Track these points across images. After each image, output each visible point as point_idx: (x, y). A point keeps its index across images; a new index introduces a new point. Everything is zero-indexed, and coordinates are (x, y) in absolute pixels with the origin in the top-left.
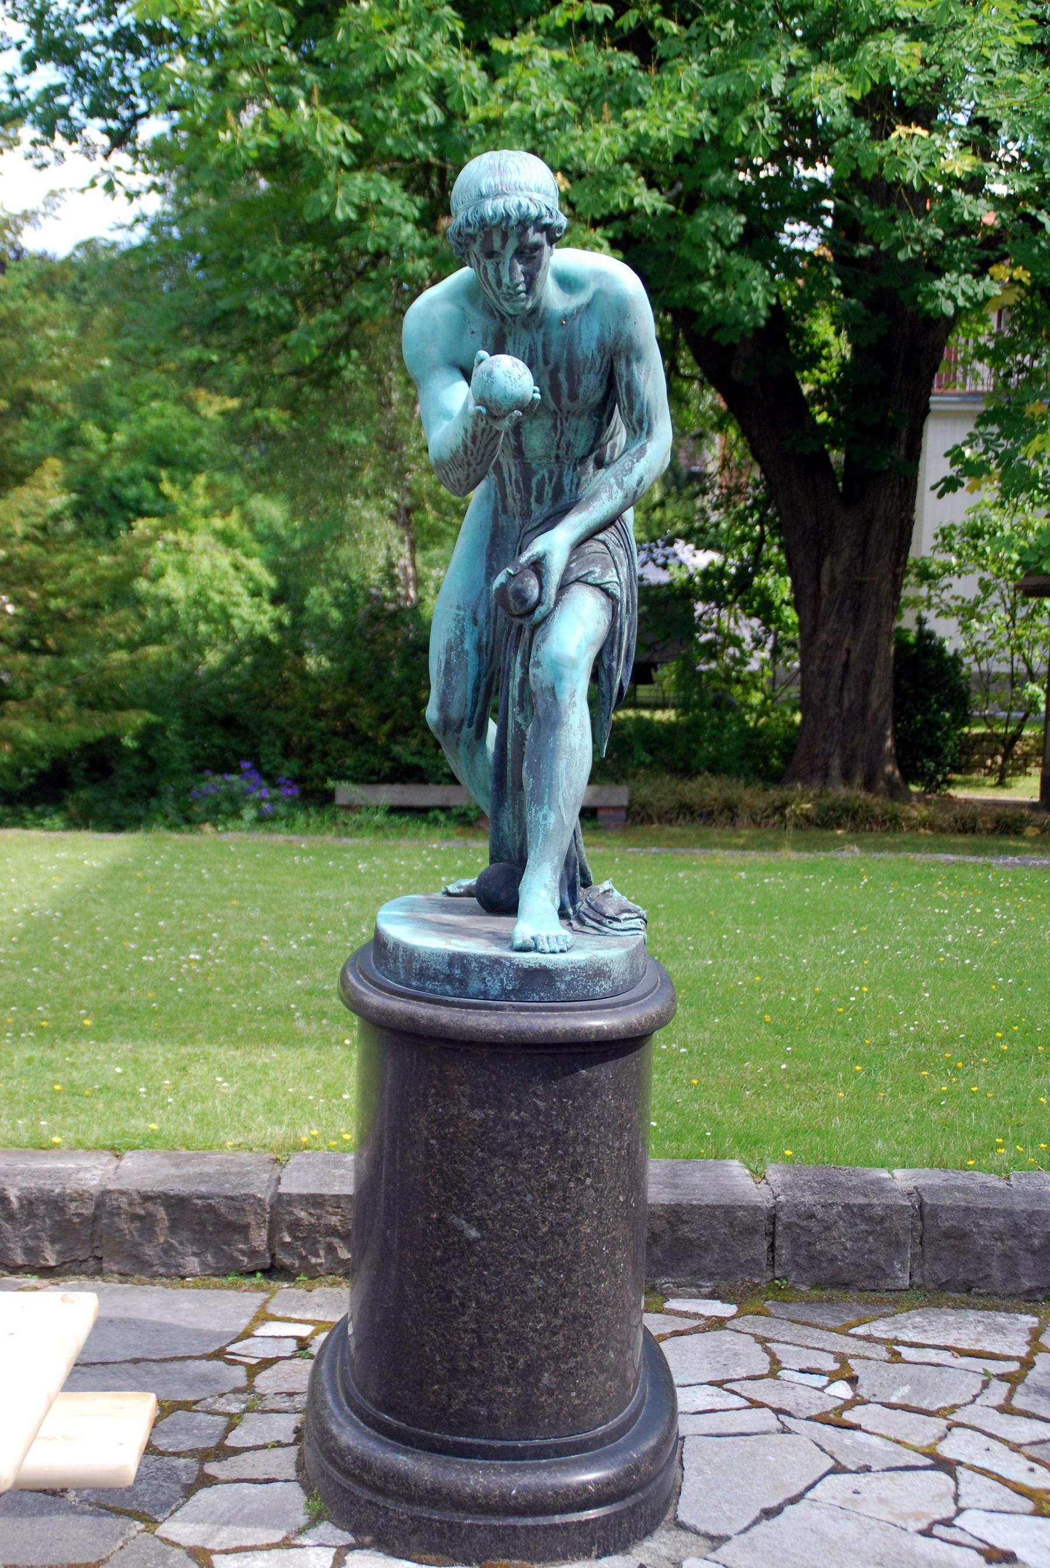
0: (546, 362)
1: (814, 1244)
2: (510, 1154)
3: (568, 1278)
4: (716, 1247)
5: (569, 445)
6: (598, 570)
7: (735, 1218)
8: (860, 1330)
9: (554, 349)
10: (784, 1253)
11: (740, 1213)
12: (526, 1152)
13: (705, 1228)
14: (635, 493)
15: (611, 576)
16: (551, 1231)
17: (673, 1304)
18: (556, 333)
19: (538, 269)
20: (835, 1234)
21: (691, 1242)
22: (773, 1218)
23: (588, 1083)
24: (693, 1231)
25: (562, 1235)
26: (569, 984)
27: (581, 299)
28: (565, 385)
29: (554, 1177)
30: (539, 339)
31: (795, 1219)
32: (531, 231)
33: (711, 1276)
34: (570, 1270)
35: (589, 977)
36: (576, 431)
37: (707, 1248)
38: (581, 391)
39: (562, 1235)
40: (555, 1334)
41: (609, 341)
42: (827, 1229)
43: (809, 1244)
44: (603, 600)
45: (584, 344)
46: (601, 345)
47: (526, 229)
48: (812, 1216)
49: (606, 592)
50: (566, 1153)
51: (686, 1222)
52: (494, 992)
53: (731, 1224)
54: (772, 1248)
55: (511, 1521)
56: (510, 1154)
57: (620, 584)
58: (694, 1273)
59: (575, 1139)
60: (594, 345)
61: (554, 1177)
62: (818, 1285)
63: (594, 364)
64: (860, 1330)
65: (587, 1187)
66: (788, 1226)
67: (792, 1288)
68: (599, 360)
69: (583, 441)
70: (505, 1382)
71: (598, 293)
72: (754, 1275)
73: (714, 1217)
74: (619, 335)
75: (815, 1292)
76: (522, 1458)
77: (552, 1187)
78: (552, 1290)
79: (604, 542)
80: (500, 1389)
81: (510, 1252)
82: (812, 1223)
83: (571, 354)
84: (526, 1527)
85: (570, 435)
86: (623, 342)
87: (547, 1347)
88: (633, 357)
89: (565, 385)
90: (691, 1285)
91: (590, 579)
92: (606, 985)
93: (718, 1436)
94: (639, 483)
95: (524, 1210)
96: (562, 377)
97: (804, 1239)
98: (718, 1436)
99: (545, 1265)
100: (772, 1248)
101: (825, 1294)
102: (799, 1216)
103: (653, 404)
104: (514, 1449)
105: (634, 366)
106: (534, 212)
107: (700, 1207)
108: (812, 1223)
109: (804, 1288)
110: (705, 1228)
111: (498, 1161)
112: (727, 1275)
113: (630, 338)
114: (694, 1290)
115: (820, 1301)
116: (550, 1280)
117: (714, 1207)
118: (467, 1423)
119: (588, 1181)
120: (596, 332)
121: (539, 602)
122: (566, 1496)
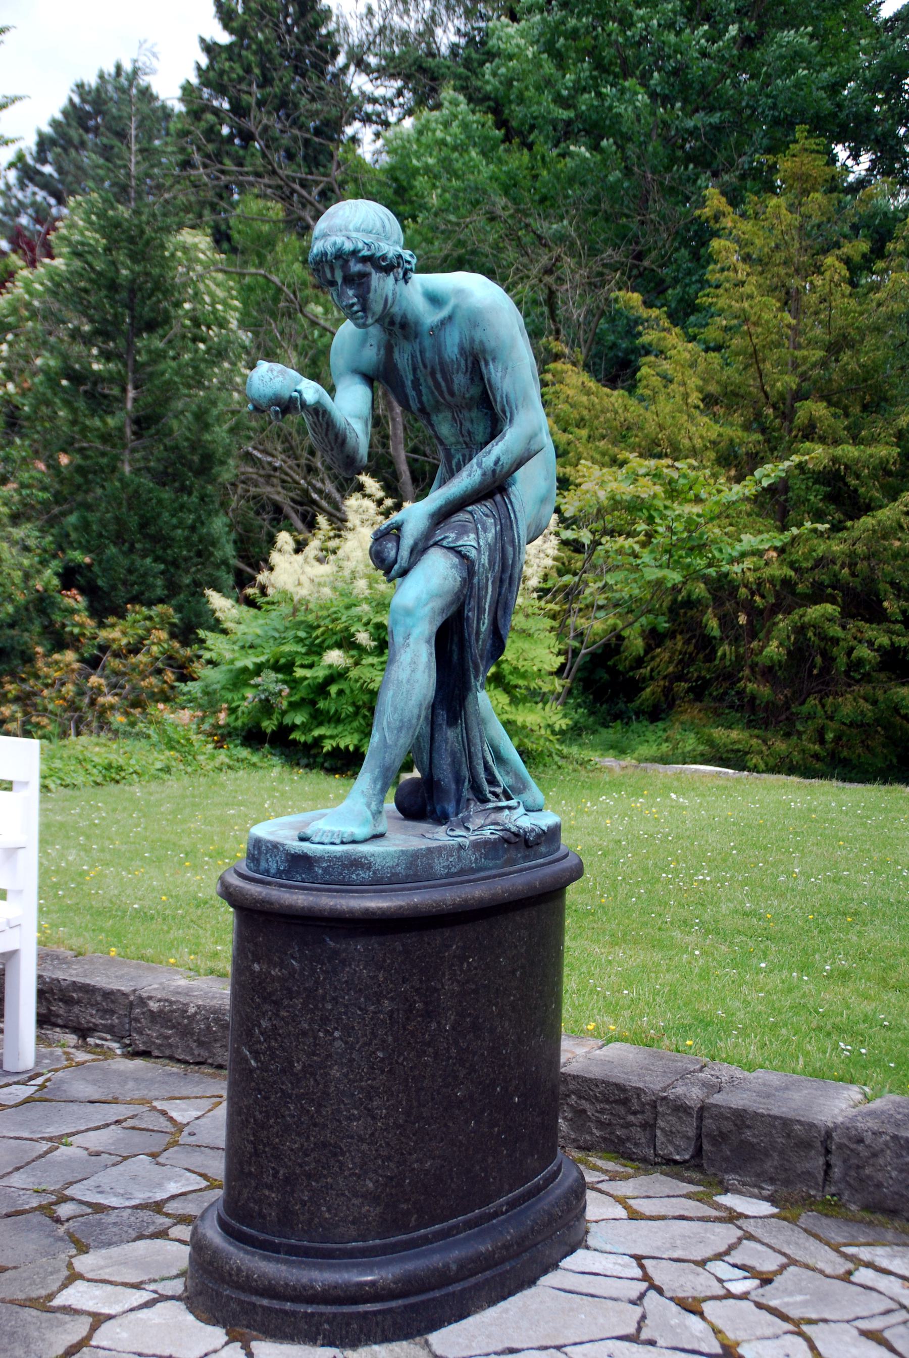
0: (425, 366)
1: (863, 1167)
2: (275, 1003)
3: (318, 1111)
4: (775, 1155)
5: (469, 433)
6: (452, 535)
7: (792, 1131)
8: (850, 1250)
9: (428, 355)
10: (837, 1172)
11: (797, 1127)
12: (286, 1002)
13: (765, 1135)
14: (494, 471)
15: (469, 540)
16: (304, 1069)
17: (728, 1200)
18: (427, 342)
19: (368, 292)
20: (881, 1161)
21: (752, 1145)
22: (828, 1135)
23: (335, 953)
24: (754, 1136)
25: (313, 1074)
26: (325, 870)
27: (444, 313)
28: (443, 384)
29: (306, 1026)
30: (417, 347)
31: (845, 1141)
32: (352, 263)
33: (772, 1181)
34: (320, 1105)
35: (344, 866)
36: (472, 421)
37: (767, 1155)
38: (456, 387)
39: (313, 1074)
40: (307, 1155)
41: (467, 345)
42: (875, 1155)
43: (858, 1167)
44: (456, 560)
45: (449, 350)
46: (462, 349)
47: (347, 261)
48: (861, 1141)
49: (458, 553)
50: (316, 1007)
51: (749, 1127)
52: (273, 871)
53: (789, 1136)
54: (828, 1166)
55: (254, 1299)
56: (275, 1003)
57: (478, 550)
58: (758, 1175)
59: (324, 997)
60: (456, 350)
61: (306, 1026)
62: (866, 1208)
63: (459, 365)
64: (850, 1250)
65: (335, 1039)
66: (841, 1146)
67: (844, 1205)
68: (463, 363)
69: (481, 429)
70: (270, 1187)
71: (456, 307)
72: (810, 1187)
73: (774, 1127)
74: (472, 340)
75: (863, 1214)
76: (278, 1252)
77: (304, 1033)
78: (304, 1118)
79: (471, 513)
80: (267, 1193)
81: (275, 1082)
82: (860, 1148)
83: (441, 358)
84: (262, 1306)
85: (467, 425)
86: (477, 346)
87: (301, 1166)
88: (489, 358)
89: (443, 384)
90: (755, 1186)
91: (445, 543)
92: (365, 875)
93: (592, 1296)
94: (496, 463)
95: (284, 1050)
96: (439, 376)
97: (854, 1161)
98: (592, 1296)
99: (300, 1097)
100: (828, 1166)
101: (867, 1216)
102: (850, 1139)
103: (512, 397)
104: (273, 1243)
105: (491, 366)
106: (348, 246)
107: (762, 1115)
108: (860, 1148)
109: (853, 1207)
110: (765, 1135)
111: (266, 1007)
112: (787, 1183)
113: (482, 343)
114: (756, 1191)
115: (861, 1221)
116: (304, 1111)
117: (775, 1118)
118: (286, 1220)
119: (337, 1034)
120: (457, 340)
121: (395, 562)
122: (294, 1288)
